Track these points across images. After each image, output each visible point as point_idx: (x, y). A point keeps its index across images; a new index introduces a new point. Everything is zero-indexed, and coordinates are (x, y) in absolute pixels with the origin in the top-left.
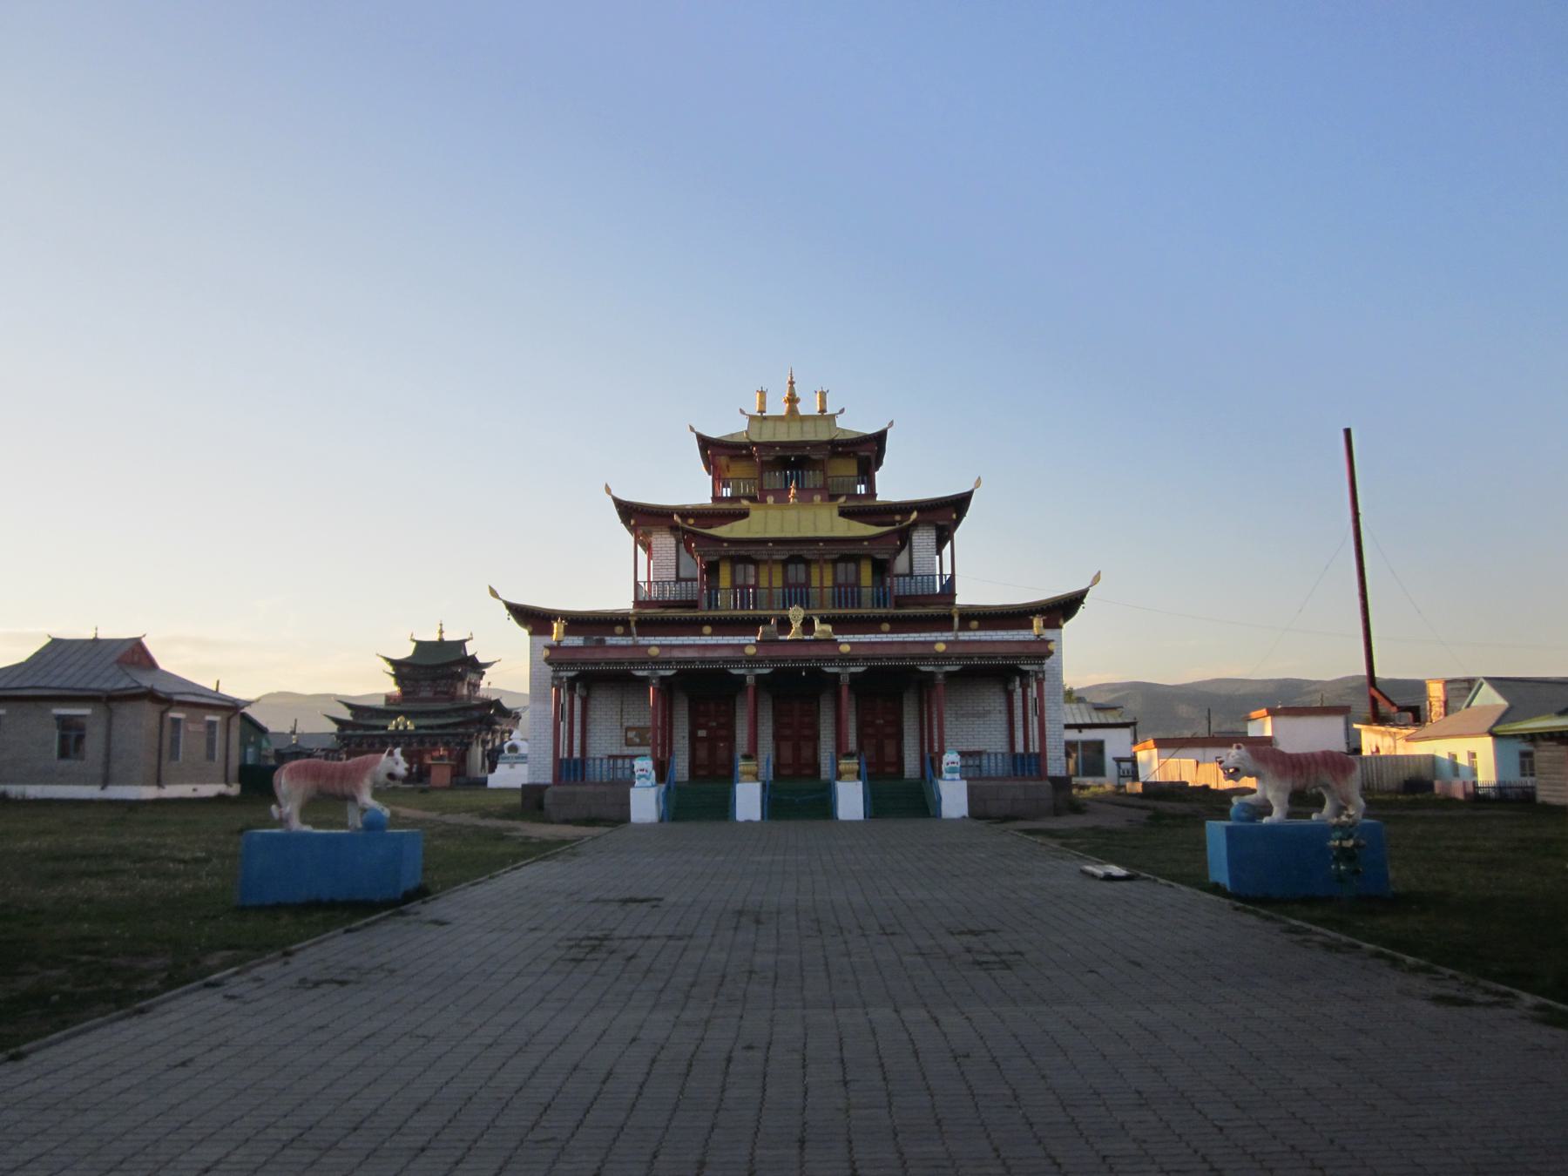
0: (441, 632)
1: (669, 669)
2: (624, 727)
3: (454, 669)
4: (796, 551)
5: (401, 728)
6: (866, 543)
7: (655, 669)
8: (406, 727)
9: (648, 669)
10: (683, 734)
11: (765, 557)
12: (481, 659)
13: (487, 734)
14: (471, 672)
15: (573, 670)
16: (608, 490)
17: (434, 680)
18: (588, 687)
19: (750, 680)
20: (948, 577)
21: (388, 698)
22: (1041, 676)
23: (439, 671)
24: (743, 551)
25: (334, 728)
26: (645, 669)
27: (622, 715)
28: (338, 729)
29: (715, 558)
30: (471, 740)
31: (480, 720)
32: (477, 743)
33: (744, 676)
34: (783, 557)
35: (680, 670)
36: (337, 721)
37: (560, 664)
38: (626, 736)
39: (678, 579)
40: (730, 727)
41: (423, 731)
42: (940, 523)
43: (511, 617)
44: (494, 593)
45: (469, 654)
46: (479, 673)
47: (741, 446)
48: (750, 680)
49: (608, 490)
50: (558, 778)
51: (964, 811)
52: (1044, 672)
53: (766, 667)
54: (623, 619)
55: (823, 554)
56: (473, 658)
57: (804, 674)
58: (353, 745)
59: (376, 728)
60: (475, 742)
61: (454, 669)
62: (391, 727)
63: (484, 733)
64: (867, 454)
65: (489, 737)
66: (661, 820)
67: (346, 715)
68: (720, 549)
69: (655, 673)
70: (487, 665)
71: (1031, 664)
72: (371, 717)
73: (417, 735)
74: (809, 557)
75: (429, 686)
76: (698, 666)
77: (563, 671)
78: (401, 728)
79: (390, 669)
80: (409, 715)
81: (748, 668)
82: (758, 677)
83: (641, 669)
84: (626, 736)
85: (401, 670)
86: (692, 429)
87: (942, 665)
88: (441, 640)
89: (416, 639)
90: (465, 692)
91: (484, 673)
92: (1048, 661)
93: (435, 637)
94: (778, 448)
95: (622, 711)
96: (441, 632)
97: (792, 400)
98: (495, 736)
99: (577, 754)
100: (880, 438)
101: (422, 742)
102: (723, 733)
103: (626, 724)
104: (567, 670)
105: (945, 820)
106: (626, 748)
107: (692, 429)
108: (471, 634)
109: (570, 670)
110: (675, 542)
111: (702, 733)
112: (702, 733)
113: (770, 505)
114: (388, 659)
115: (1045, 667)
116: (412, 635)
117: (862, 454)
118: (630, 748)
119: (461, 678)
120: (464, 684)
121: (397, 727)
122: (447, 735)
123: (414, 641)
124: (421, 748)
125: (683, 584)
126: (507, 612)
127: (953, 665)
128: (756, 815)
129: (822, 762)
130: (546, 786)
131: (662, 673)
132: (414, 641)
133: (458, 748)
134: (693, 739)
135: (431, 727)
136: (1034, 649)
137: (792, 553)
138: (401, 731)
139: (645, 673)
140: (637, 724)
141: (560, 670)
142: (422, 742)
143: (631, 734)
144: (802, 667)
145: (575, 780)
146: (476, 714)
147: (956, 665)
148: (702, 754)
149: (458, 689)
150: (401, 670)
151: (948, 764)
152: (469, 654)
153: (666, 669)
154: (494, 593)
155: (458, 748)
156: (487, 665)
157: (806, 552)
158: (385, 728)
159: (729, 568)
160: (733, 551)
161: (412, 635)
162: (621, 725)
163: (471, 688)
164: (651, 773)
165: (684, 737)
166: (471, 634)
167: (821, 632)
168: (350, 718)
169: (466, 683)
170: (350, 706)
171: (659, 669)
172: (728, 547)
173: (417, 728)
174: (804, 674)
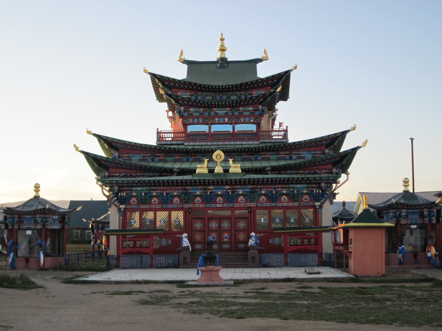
0: (223, 50)
5: (219, 169)
23: (234, 98)
41: (248, 176)
58: (134, 200)
75: (226, 115)
78: (219, 169)
89: (187, 58)
96: (223, 50)
108: (265, 52)
116: (182, 53)
121: (211, 171)
123: (185, 62)
124: (253, 205)
132: (185, 62)
135: (262, 171)
138: (219, 174)
158: (192, 172)
161: (182, 53)
166: (265, 52)
173: (245, 171)
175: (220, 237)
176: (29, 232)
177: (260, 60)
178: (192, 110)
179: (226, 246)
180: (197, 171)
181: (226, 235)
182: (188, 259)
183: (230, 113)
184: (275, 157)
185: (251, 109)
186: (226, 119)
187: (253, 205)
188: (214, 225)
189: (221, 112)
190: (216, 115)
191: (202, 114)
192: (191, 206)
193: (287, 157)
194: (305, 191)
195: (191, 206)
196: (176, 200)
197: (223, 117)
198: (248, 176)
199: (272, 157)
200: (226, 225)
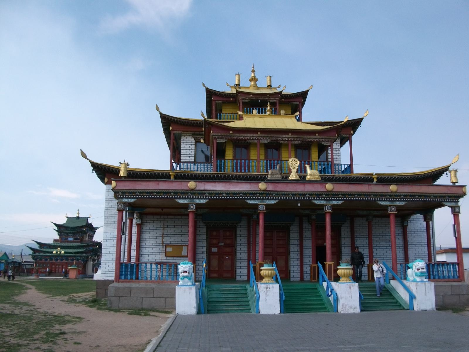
0: (78, 214)
1: (203, 199)
2: (164, 245)
3: (83, 229)
4: (274, 137)
6: (317, 135)
7: (193, 198)
8: (60, 253)
9: (188, 198)
10: (203, 250)
11: (256, 141)
12: (94, 226)
13: (96, 257)
14: (90, 230)
15: (133, 198)
16: (158, 109)
17: (74, 233)
18: (142, 216)
19: (262, 208)
20: (346, 166)
21: (55, 241)
22: (457, 210)
24: (242, 136)
25: (31, 252)
26: (185, 198)
27: (163, 237)
28: (33, 253)
29: (225, 141)
30: (88, 259)
31: (92, 251)
32: (91, 260)
33: (257, 205)
34: (267, 142)
35: (210, 199)
36: (32, 249)
37: (124, 193)
38: (166, 250)
39: (195, 162)
40: (233, 246)
41: (67, 255)
42: (345, 136)
43: (94, 171)
44: (84, 155)
45: (89, 223)
46: (93, 231)
47: (230, 95)
48: (262, 208)
49: (158, 109)
50: (119, 277)
51: (434, 306)
52: (459, 207)
53: (273, 199)
54: (166, 175)
55: (291, 141)
56: (91, 224)
57: (299, 205)
58: (38, 260)
59: (48, 252)
60: (90, 260)
61: (83, 229)
62: (54, 252)
63: (94, 256)
64: (298, 103)
65: (96, 258)
66: (199, 312)
67: (37, 247)
68: (228, 134)
69: (193, 202)
70: (97, 228)
71: (451, 202)
72: (47, 248)
73: (65, 256)
74: (282, 142)
75: (72, 236)
76: (224, 196)
77: (126, 198)
79: (56, 228)
80: (62, 247)
81: (260, 199)
82: (267, 206)
83: (183, 198)
84: (166, 250)
85: (60, 228)
86: (204, 85)
87: (394, 201)
88: (78, 218)
90: (87, 239)
91: (95, 232)
92: (461, 200)
93: (76, 216)
94: (251, 95)
95: (163, 234)
97: (254, 79)
98: (98, 258)
99: (133, 260)
100: (303, 95)
101: (67, 259)
102: (228, 250)
103: (166, 243)
104: (128, 198)
105: (418, 312)
106: (165, 258)
107: (204, 85)
109: (131, 198)
110: (194, 142)
111: (214, 250)
112: (214, 250)
113: (254, 115)
114: (56, 225)
115: (459, 204)
116: (66, 215)
117: (294, 103)
118: (168, 258)
119: (85, 233)
120: (86, 235)
121: (57, 253)
122: (78, 256)
123: (67, 217)
124: (67, 262)
125: (199, 165)
126: (92, 168)
127: (401, 201)
128: (275, 308)
129: (291, 269)
130: (112, 282)
131: (198, 201)
132: (67, 217)
133: (82, 262)
134: (209, 254)
136: (454, 191)
137: (272, 139)
139: (185, 201)
140: (173, 243)
141: (123, 198)
142: (67, 259)
143: (169, 249)
144: (299, 200)
145: (132, 279)
146: (91, 248)
147: (403, 201)
148: (215, 263)
149: (84, 238)
150: (60, 228)
151: (418, 269)
152: (89, 223)
153: (201, 199)
154: (84, 155)
155: (82, 262)
156: (97, 228)
157: (282, 139)
158: (52, 252)
159: (232, 149)
160: (236, 136)
161: (66, 215)
162: (162, 244)
163: (89, 237)
164: (191, 275)
165: (203, 252)
167: (311, 175)
168: (39, 248)
169: (88, 235)
170: (38, 243)
171: (196, 198)
172: (232, 133)
173: (65, 253)
174: (299, 205)
175: (58, 269)
176: (10, 267)
177: (89, 217)
178: (63, 234)
179: (60, 272)
180: (54, 253)
181: (60, 269)
182: (48, 275)
183: (73, 235)
184: (82, 248)
185: (78, 234)
186: (72, 237)
187: (67, 262)
188: (57, 266)
189: (70, 235)
190: (69, 235)
191: (65, 235)
192: (52, 261)
193: (85, 248)
194: (80, 259)
195: (52, 261)
196: (48, 260)
197: (71, 236)
198: (67, 255)
199: (81, 248)
200: (60, 266)
